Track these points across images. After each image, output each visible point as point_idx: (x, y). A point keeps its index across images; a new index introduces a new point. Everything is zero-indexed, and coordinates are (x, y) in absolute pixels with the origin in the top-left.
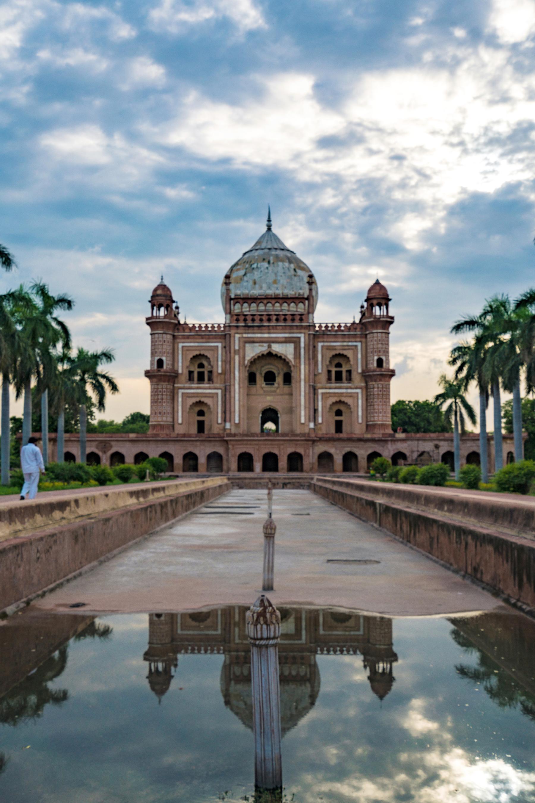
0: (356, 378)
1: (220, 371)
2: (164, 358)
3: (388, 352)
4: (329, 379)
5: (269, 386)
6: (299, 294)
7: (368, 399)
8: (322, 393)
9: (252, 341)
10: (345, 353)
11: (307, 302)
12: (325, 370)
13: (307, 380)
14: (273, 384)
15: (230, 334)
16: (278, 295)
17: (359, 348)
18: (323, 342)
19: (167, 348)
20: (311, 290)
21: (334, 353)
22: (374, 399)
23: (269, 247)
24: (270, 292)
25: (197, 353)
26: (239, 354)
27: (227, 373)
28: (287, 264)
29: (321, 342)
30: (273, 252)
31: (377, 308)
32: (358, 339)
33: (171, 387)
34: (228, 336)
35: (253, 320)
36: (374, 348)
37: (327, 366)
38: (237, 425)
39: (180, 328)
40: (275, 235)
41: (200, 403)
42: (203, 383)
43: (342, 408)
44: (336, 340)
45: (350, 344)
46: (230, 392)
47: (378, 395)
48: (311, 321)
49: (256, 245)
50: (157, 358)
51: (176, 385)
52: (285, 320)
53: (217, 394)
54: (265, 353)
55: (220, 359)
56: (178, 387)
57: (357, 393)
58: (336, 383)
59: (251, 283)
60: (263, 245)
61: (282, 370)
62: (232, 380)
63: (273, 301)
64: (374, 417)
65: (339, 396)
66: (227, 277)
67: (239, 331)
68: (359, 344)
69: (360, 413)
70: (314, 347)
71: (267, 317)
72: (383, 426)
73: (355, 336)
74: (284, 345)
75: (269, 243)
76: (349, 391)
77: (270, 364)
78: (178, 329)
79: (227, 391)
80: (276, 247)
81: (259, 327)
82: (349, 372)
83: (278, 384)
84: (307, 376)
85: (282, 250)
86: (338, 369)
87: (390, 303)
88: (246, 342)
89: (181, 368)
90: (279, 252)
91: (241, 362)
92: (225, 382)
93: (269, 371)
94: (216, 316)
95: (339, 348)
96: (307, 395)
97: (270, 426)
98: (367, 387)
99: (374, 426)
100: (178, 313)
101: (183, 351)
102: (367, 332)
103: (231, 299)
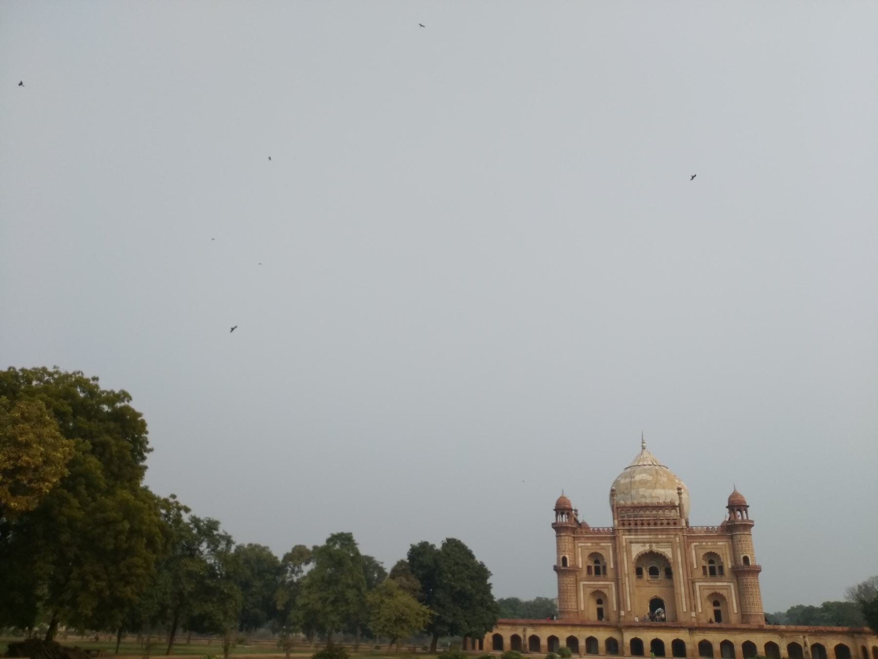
1: (612, 566)
2: (567, 556)
3: (752, 551)
4: (705, 573)
10: (716, 551)
20: (680, 498)
31: (739, 513)
39: (579, 530)
43: (719, 600)
50: (561, 556)
66: (612, 490)
82: (721, 568)
87: (748, 509)
88: (631, 542)
89: (582, 562)
100: (577, 515)
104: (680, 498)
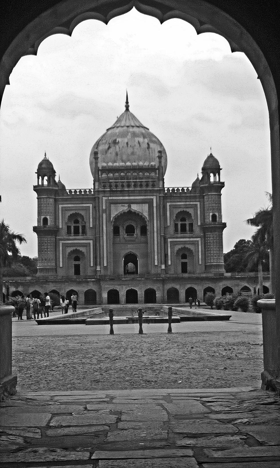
0: (197, 230)
1: (91, 226)
2: (48, 217)
4: (176, 230)
6: (152, 165)
7: (205, 245)
8: (171, 242)
9: (116, 203)
10: (188, 210)
11: (157, 171)
12: (172, 222)
13: (159, 231)
16: (135, 166)
17: (199, 206)
18: (171, 202)
19: (51, 208)
20: (160, 162)
21: (180, 210)
22: (210, 245)
23: (127, 125)
24: (128, 164)
26: (106, 213)
27: (97, 227)
28: (141, 140)
29: (168, 202)
30: (131, 129)
31: (212, 175)
32: (198, 200)
35: (116, 186)
36: (209, 207)
37: (174, 221)
38: (106, 268)
40: (132, 114)
41: (76, 251)
42: (79, 236)
43: (186, 253)
45: (191, 203)
47: (213, 242)
48: (161, 186)
49: (117, 122)
50: (43, 217)
52: (141, 186)
55: (91, 217)
58: (181, 234)
59: (114, 154)
60: (123, 124)
62: (101, 234)
63: (132, 172)
64: (211, 259)
68: (198, 203)
69: (200, 257)
70: (164, 206)
71: (127, 183)
72: (218, 266)
73: (195, 197)
75: (127, 120)
76: (192, 239)
77: (130, 219)
78: (58, 194)
79: (97, 241)
80: (133, 124)
81: (121, 191)
82: (191, 225)
84: (159, 228)
85: (138, 127)
90: (136, 130)
91: (108, 219)
92: (95, 235)
93: (130, 225)
94: (86, 182)
95: (183, 206)
97: (130, 265)
98: (205, 237)
99: (211, 266)
101: (62, 210)
103: (99, 170)
104: (160, 162)
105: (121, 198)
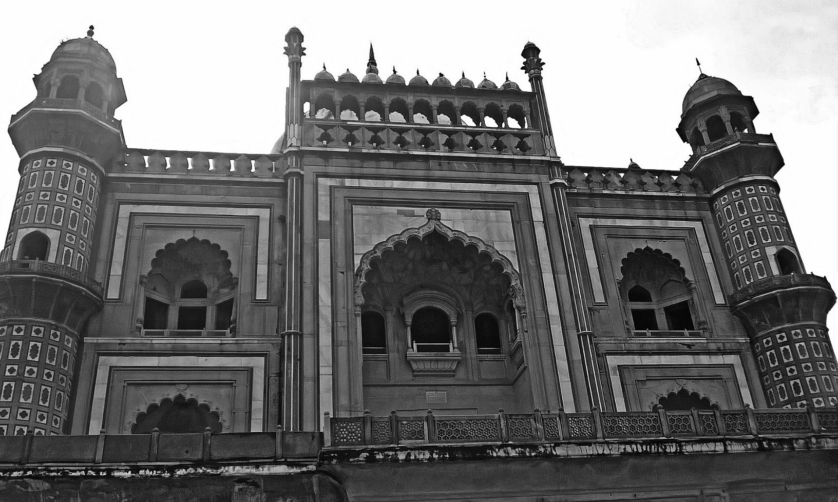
1: (262, 295)
2: (53, 235)
5: (431, 355)
10: (663, 247)
13: (569, 317)
14: (447, 349)
15: (301, 177)
17: (701, 235)
22: (801, 376)
25: (186, 235)
32: (692, 213)
33: (70, 343)
34: (292, 183)
42: (199, 335)
44: (630, 211)
46: (300, 360)
50: (23, 233)
51: (87, 340)
53: (250, 371)
54: (421, 234)
55: (263, 257)
56: (97, 344)
57: (731, 366)
61: (469, 304)
62: (308, 318)
65: (673, 379)
66: (295, 37)
67: (331, 170)
68: (697, 226)
74: (481, 213)
76: (704, 360)
83: (462, 347)
84: (567, 306)
86: (641, 306)
88: (354, 201)
91: (341, 260)
96: (578, 368)
102: (715, 192)
104: (536, 80)
105: (397, 184)
